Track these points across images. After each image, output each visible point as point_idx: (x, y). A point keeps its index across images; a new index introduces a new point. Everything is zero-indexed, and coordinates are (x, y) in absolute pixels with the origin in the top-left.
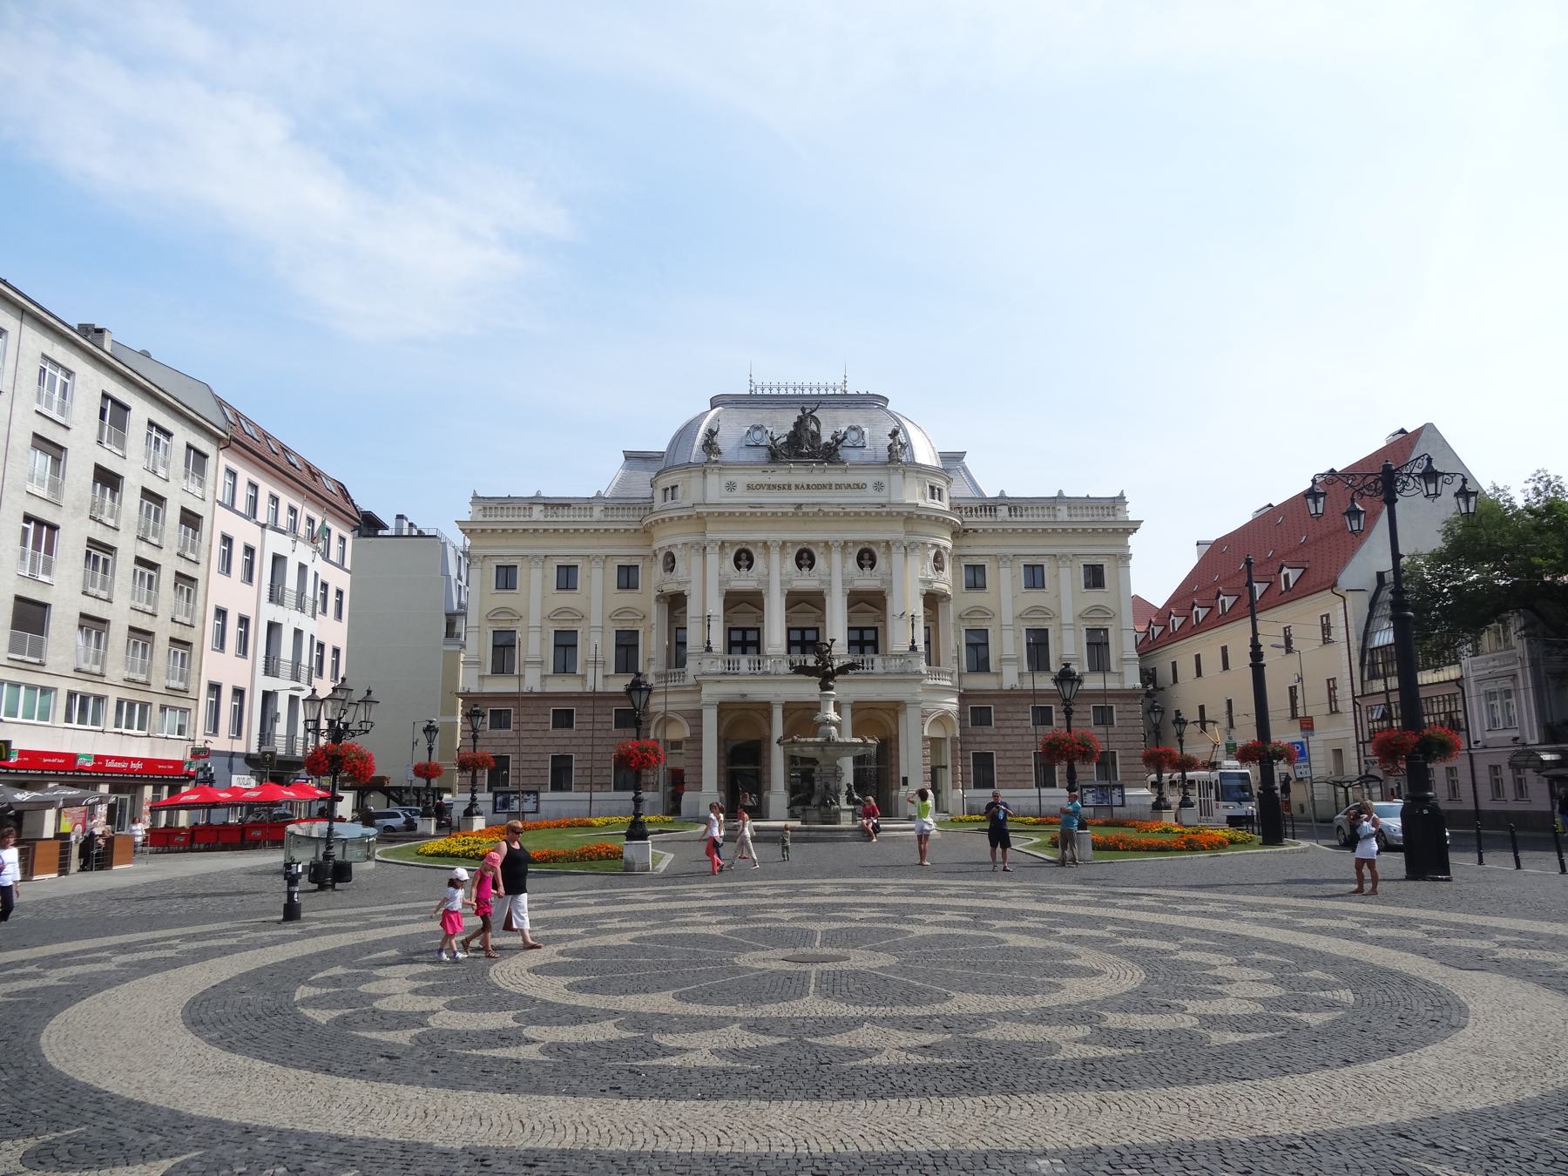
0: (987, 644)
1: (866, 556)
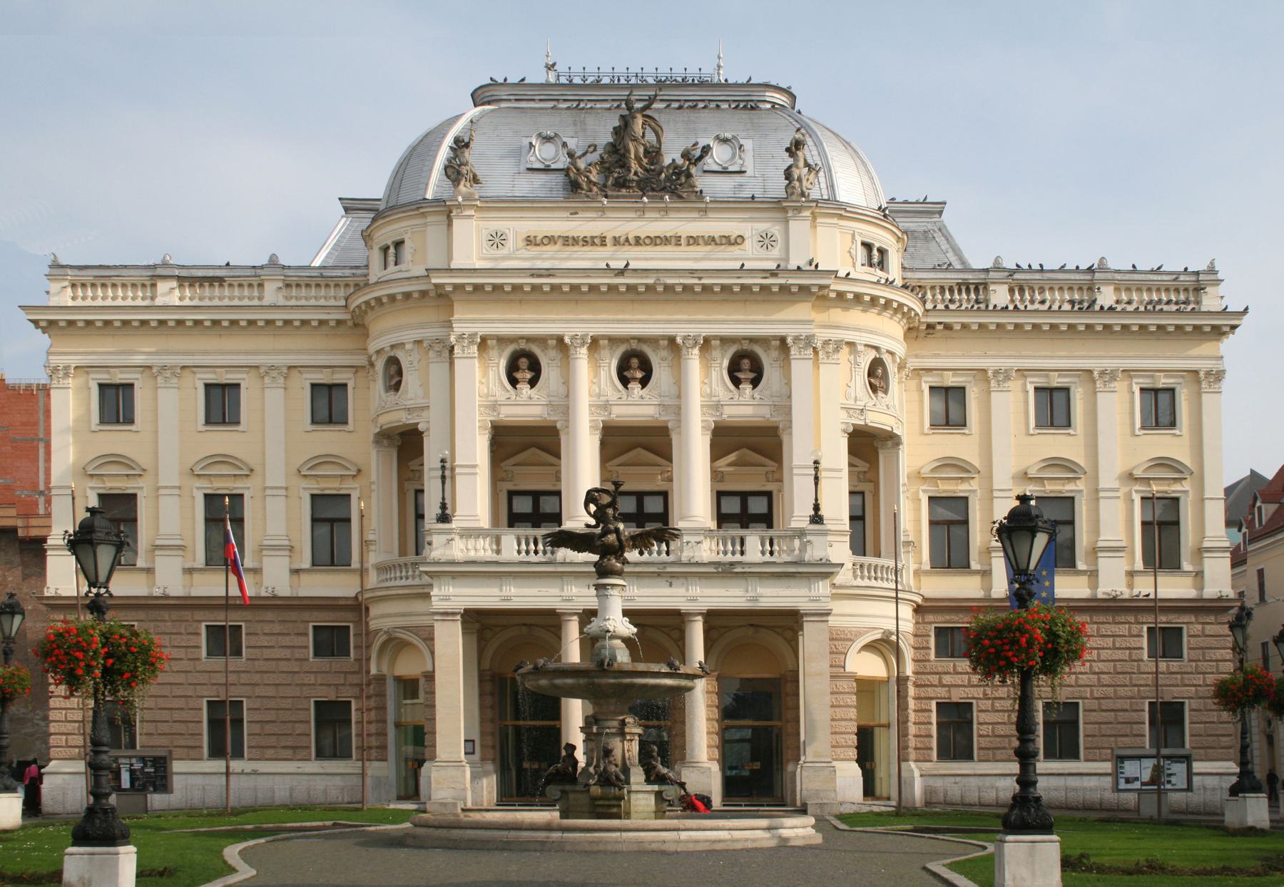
0: (965, 523)
1: (746, 363)
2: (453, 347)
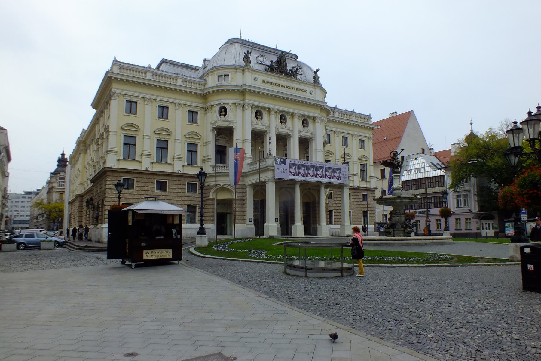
2: (243, 107)
